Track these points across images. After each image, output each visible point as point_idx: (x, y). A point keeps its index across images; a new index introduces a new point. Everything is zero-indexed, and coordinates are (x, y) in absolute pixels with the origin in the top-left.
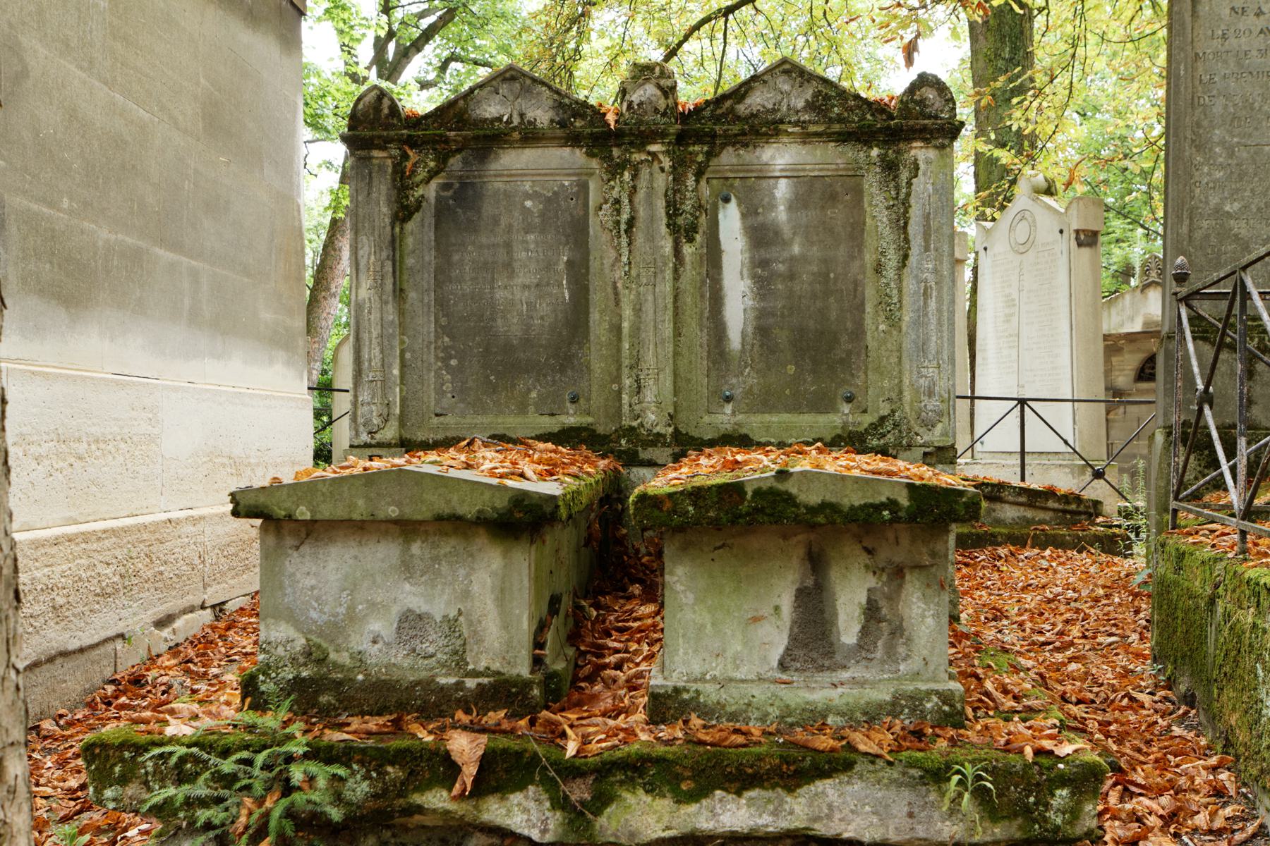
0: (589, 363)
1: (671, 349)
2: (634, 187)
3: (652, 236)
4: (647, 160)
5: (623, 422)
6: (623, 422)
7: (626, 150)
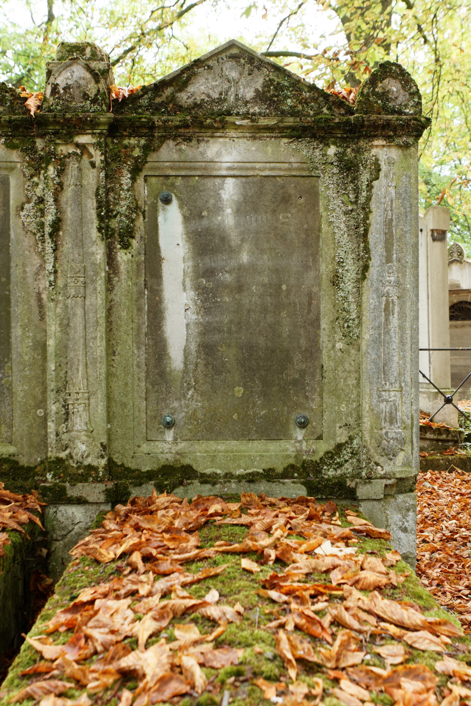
0: (11, 385)
1: (103, 370)
2: (61, 185)
3: (82, 241)
4: (75, 154)
5: (49, 454)
6: (49, 454)
7: (51, 141)
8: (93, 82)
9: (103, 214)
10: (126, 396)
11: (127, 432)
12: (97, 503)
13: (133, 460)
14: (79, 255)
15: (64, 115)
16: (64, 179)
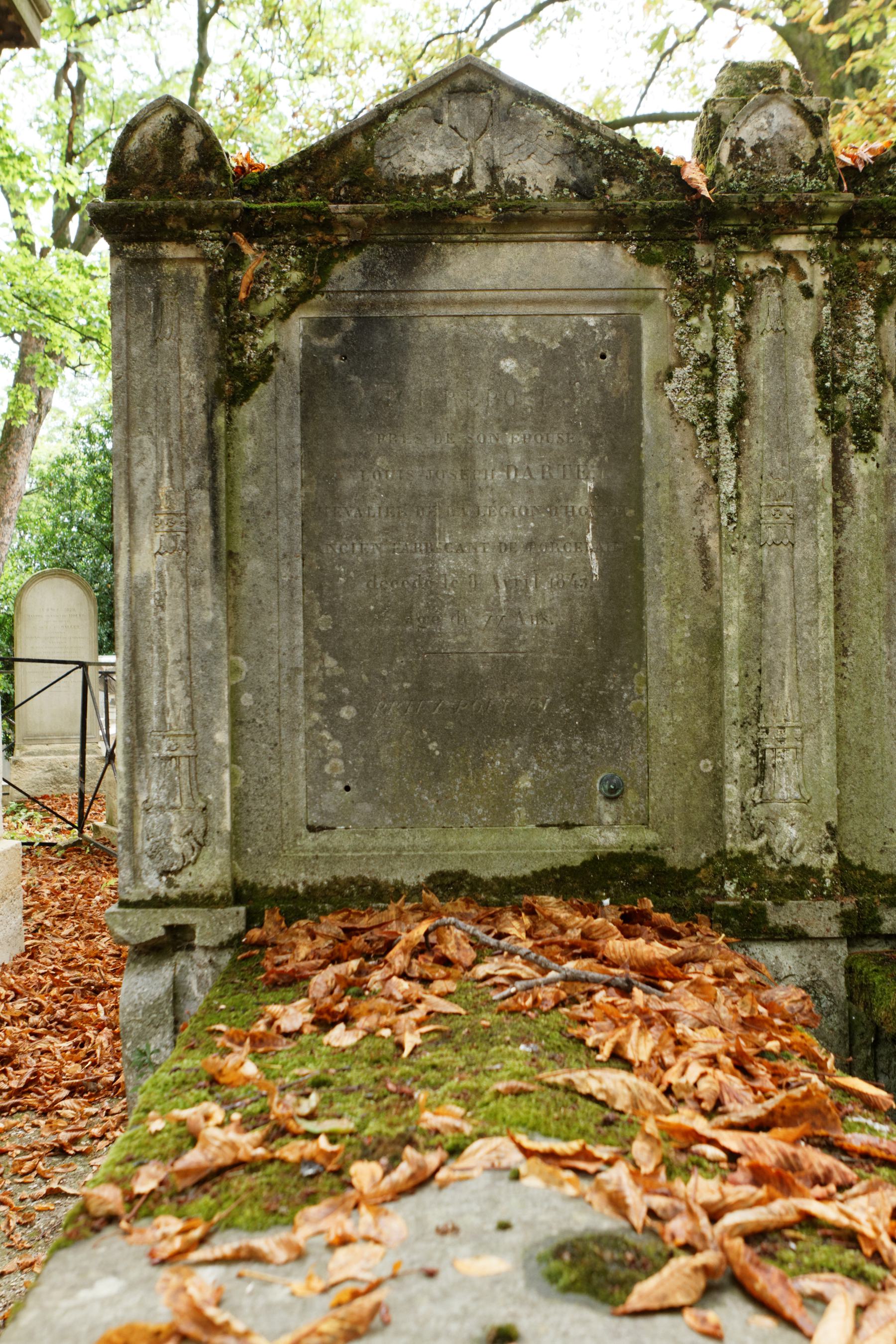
0: (646, 713)
1: (831, 685)
2: (746, 331)
3: (787, 437)
4: (773, 271)
5: (729, 845)
6: (729, 845)
7: (730, 248)
8: (808, 134)
9: (828, 384)
10: (869, 733)
11: (871, 802)
12: (822, 939)
13: (883, 857)
14: (783, 464)
15: (762, 197)
16: (752, 320)
